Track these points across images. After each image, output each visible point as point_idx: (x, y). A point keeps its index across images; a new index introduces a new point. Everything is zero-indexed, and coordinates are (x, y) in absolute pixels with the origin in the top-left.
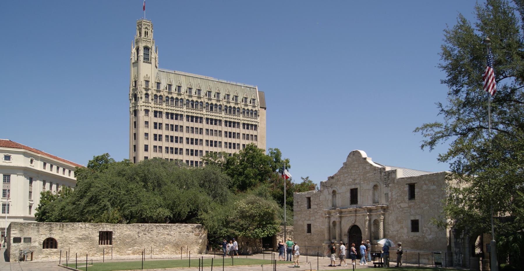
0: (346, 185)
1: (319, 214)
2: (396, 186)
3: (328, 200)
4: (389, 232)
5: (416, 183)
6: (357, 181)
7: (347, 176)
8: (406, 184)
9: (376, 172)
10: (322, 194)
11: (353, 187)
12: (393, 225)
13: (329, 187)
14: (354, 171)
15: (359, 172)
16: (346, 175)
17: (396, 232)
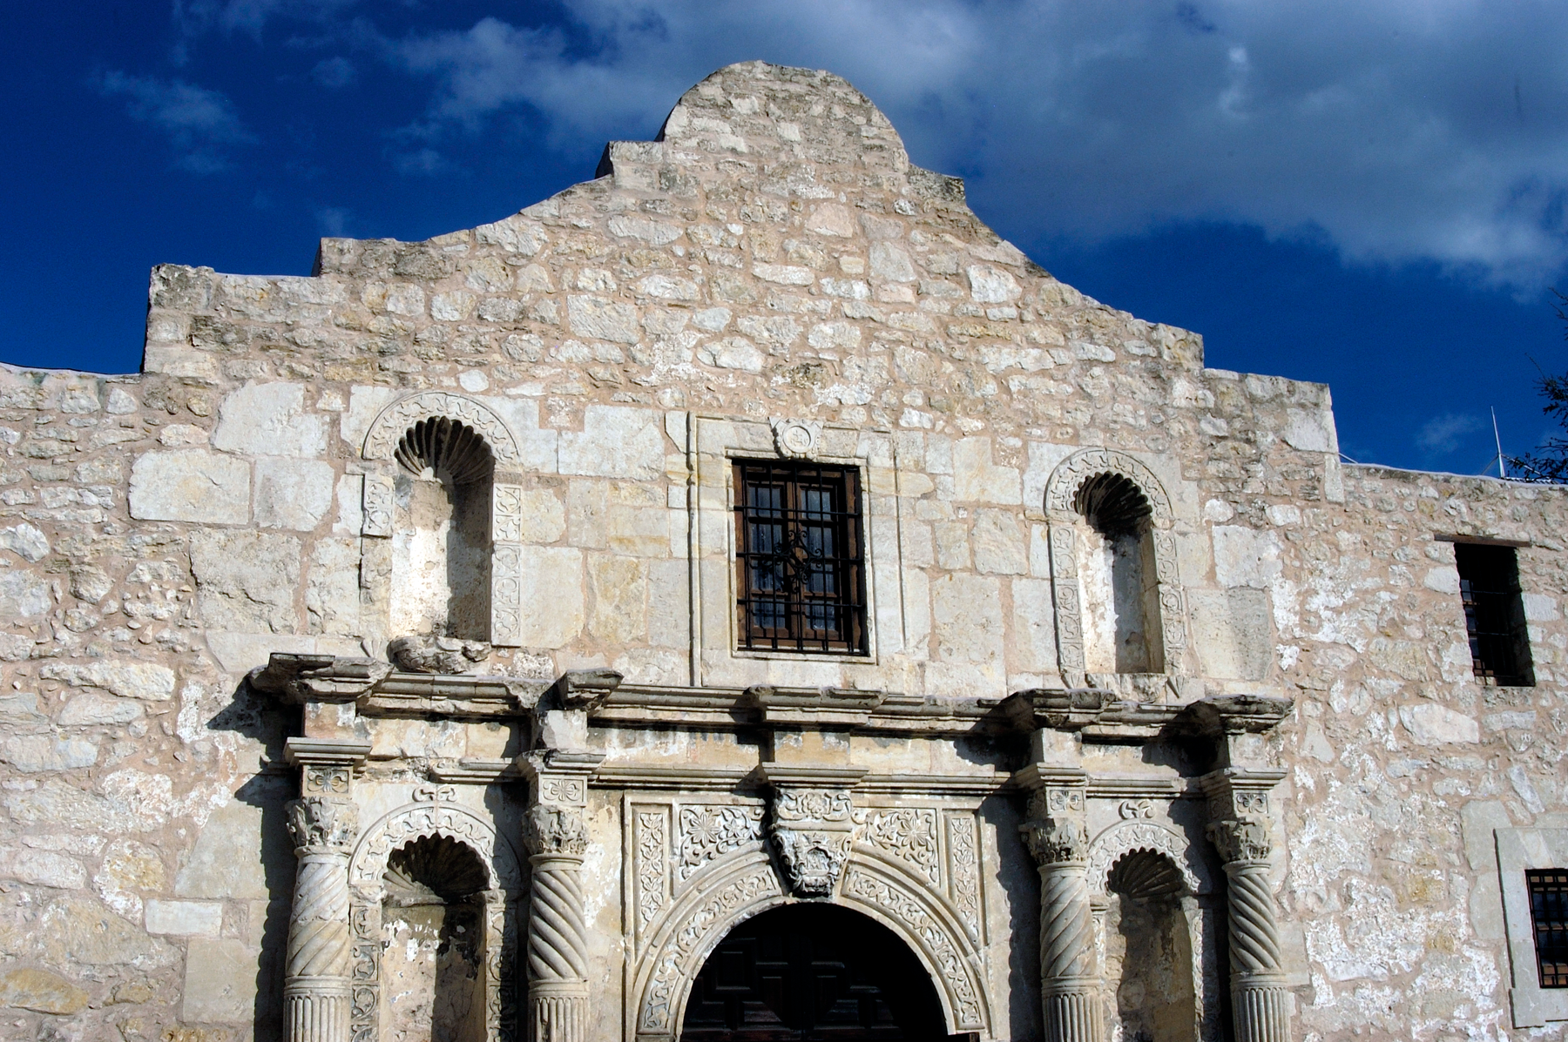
0: (668, 397)
1: (91, 709)
2: (1344, 538)
3: (308, 541)
4: (1305, 993)
5: (1527, 544)
6: (847, 393)
7: (680, 305)
8: (1440, 537)
9: (1110, 356)
10: (171, 432)
11: (800, 443)
12: (1344, 922)
13: (331, 371)
14: (796, 275)
15: (873, 300)
16: (656, 286)
17: (1386, 996)
